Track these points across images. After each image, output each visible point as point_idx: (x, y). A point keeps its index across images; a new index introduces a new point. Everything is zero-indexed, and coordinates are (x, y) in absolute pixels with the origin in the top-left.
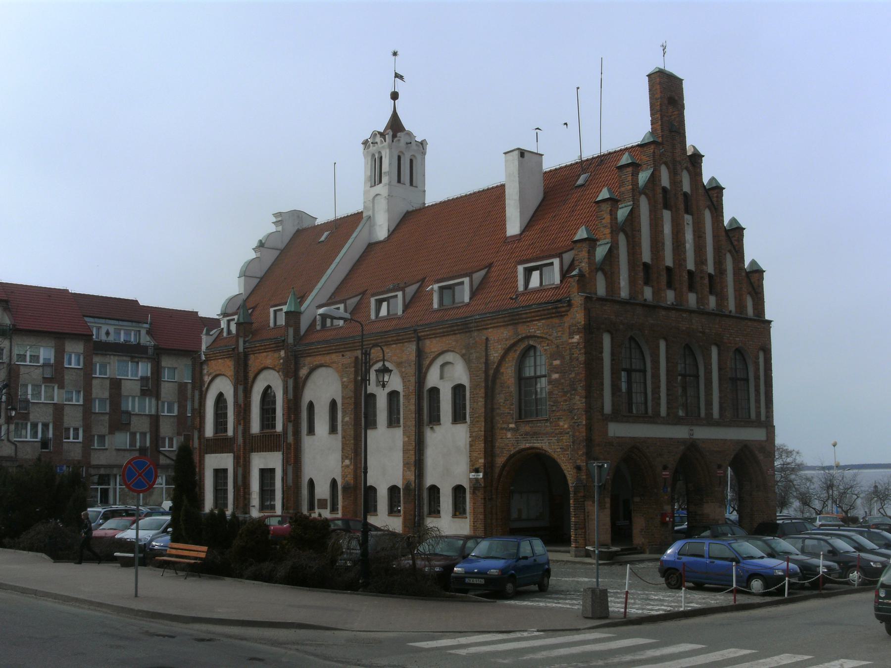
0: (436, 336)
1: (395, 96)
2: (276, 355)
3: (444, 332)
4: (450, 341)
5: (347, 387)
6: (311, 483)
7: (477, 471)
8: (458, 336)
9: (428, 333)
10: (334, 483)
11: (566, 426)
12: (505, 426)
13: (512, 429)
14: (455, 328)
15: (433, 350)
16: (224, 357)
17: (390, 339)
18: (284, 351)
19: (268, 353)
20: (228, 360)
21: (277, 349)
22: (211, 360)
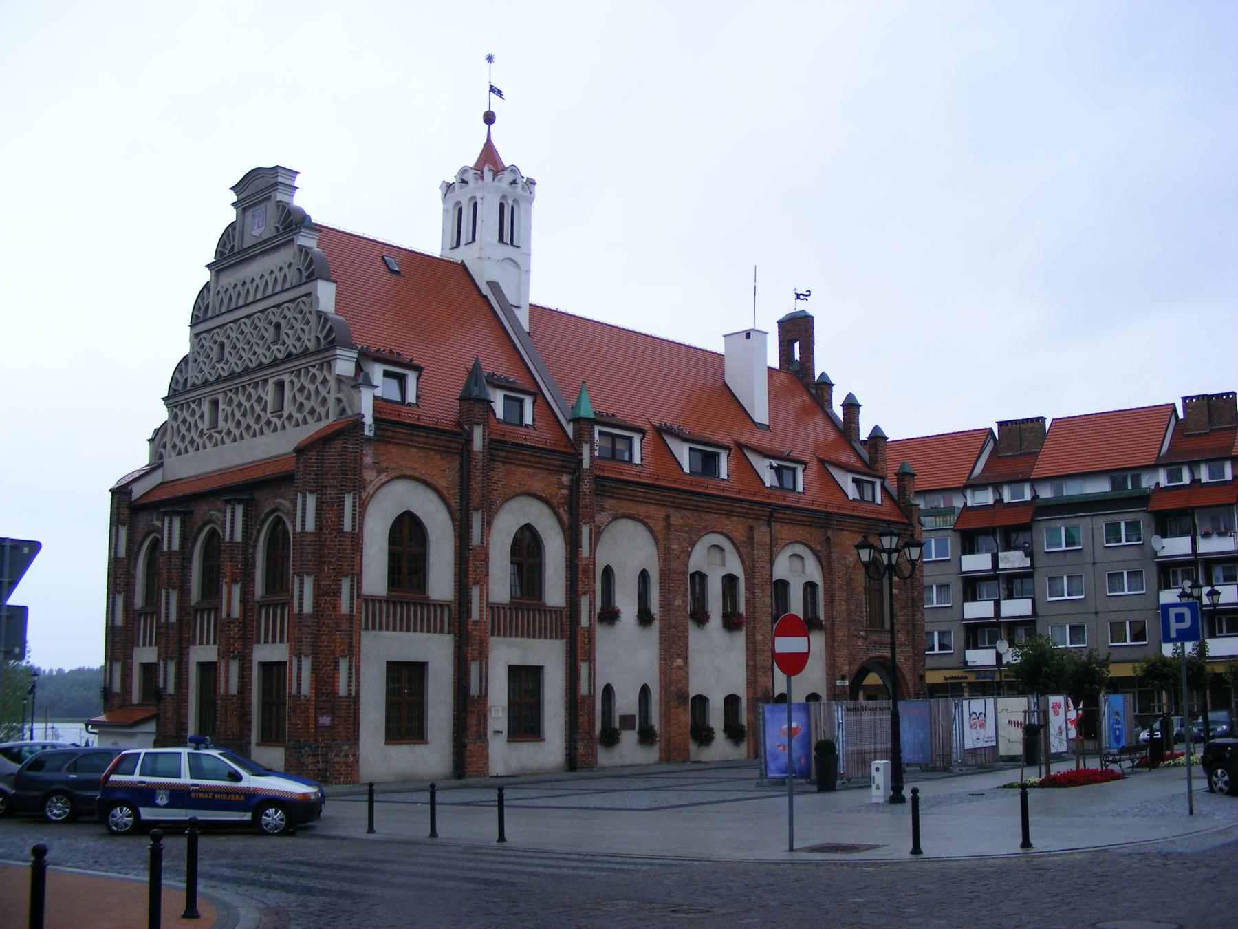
0: (792, 522)
1: (489, 118)
2: (553, 479)
3: (800, 521)
4: (803, 532)
5: (678, 558)
6: (608, 691)
7: (843, 678)
8: (812, 529)
9: (786, 516)
10: (645, 691)
11: (903, 639)
12: (855, 633)
13: (862, 636)
14: (816, 520)
15: (783, 537)
16: (434, 447)
17: (737, 509)
18: (570, 477)
19: (540, 471)
20: (438, 457)
21: (560, 471)
22: (389, 442)
